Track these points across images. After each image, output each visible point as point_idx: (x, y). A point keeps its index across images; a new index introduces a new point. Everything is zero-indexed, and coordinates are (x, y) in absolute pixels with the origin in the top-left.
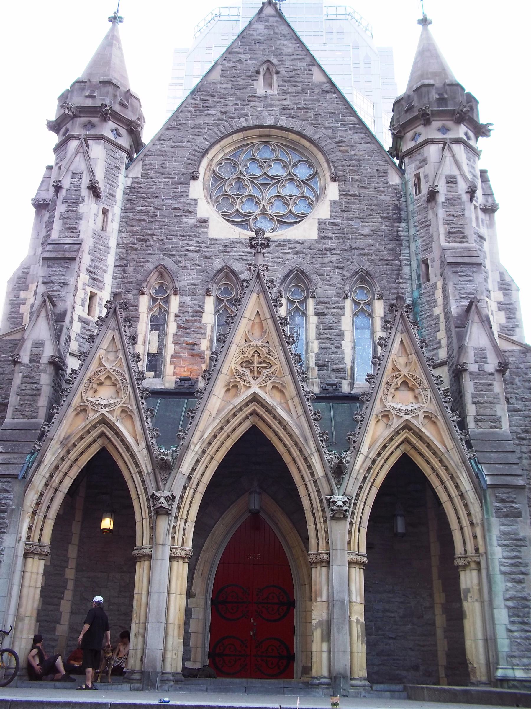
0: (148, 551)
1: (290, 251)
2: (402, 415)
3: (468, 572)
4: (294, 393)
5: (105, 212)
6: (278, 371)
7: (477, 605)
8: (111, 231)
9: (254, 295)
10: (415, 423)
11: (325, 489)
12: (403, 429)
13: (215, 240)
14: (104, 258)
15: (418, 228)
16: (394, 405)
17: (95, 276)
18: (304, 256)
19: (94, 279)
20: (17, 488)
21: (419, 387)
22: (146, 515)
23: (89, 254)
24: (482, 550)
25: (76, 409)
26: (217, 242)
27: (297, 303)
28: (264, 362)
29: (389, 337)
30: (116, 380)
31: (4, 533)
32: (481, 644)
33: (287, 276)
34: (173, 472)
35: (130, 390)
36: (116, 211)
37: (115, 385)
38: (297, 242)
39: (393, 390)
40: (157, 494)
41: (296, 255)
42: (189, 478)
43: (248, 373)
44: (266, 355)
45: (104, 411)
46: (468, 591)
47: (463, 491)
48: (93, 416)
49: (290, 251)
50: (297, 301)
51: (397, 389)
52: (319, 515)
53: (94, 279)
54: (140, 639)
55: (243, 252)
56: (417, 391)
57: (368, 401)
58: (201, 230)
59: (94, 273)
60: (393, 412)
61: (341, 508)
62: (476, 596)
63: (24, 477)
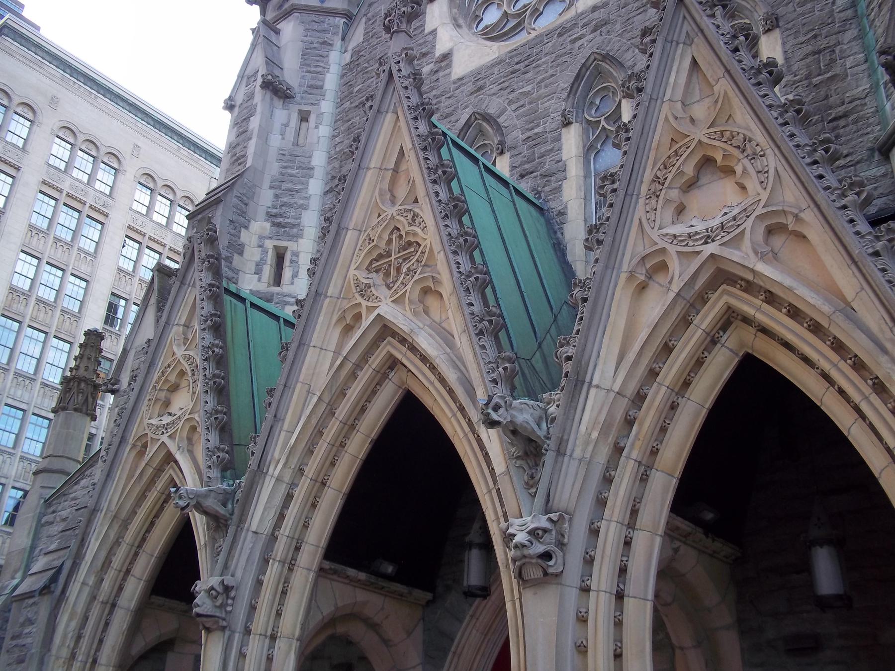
1: (584, 31)
2: (698, 249)
5: (304, 117)
6: (427, 253)
8: (315, 141)
9: (389, 118)
10: (734, 255)
11: (511, 505)
12: (713, 284)
13: (461, 79)
14: (298, 187)
16: (679, 229)
17: (281, 220)
18: (609, 27)
19: (279, 225)
20: (44, 606)
21: (741, 156)
23: (271, 188)
25: (134, 446)
26: (464, 81)
27: (603, 123)
28: (410, 244)
29: (648, 66)
33: (578, 77)
34: (231, 530)
36: (327, 106)
38: (595, 8)
39: (674, 194)
41: (595, 33)
42: (273, 538)
43: (378, 278)
44: (408, 228)
49: (584, 31)
50: (602, 118)
51: (691, 185)
53: (279, 225)
55: (504, 77)
56: (739, 169)
57: (600, 242)
58: (441, 74)
59: (281, 215)
60: (672, 249)
61: (526, 552)
63: (45, 590)
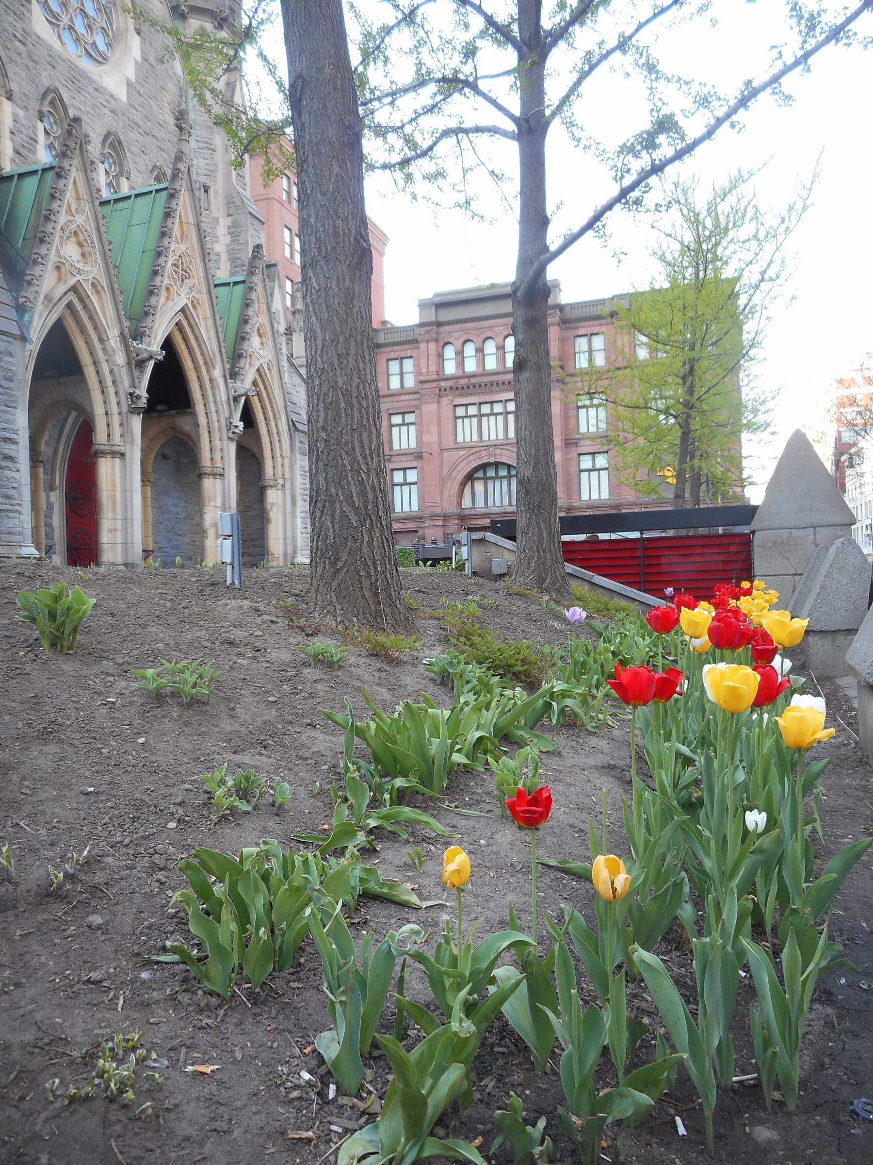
0: (122, 449)
3: (274, 489)
4: (208, 313)
7: (280, 515)
15: (201, 145)
22: (115, 410)
24: (287, 476)
30: (85, 240)
31: (16, 408)
32: (281, 541)
35: (99, 260)
37: (80, 245)
40: (137, 392)
45: (79, 277)
46: (273, 504)
47: (281, 430)
48: (72, 282)
52: (216, 436)
54: (119, 535)
62: (281, 508)
